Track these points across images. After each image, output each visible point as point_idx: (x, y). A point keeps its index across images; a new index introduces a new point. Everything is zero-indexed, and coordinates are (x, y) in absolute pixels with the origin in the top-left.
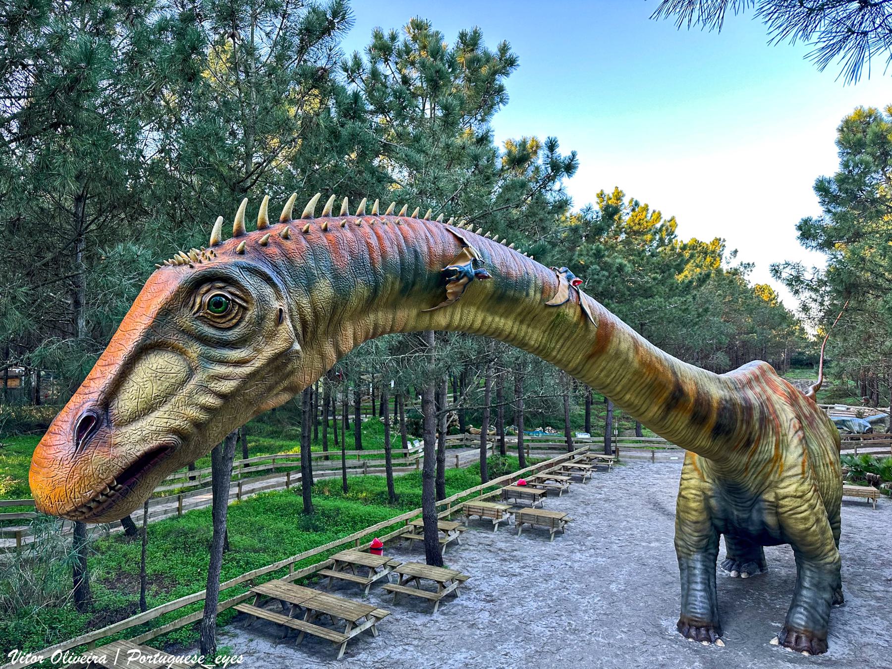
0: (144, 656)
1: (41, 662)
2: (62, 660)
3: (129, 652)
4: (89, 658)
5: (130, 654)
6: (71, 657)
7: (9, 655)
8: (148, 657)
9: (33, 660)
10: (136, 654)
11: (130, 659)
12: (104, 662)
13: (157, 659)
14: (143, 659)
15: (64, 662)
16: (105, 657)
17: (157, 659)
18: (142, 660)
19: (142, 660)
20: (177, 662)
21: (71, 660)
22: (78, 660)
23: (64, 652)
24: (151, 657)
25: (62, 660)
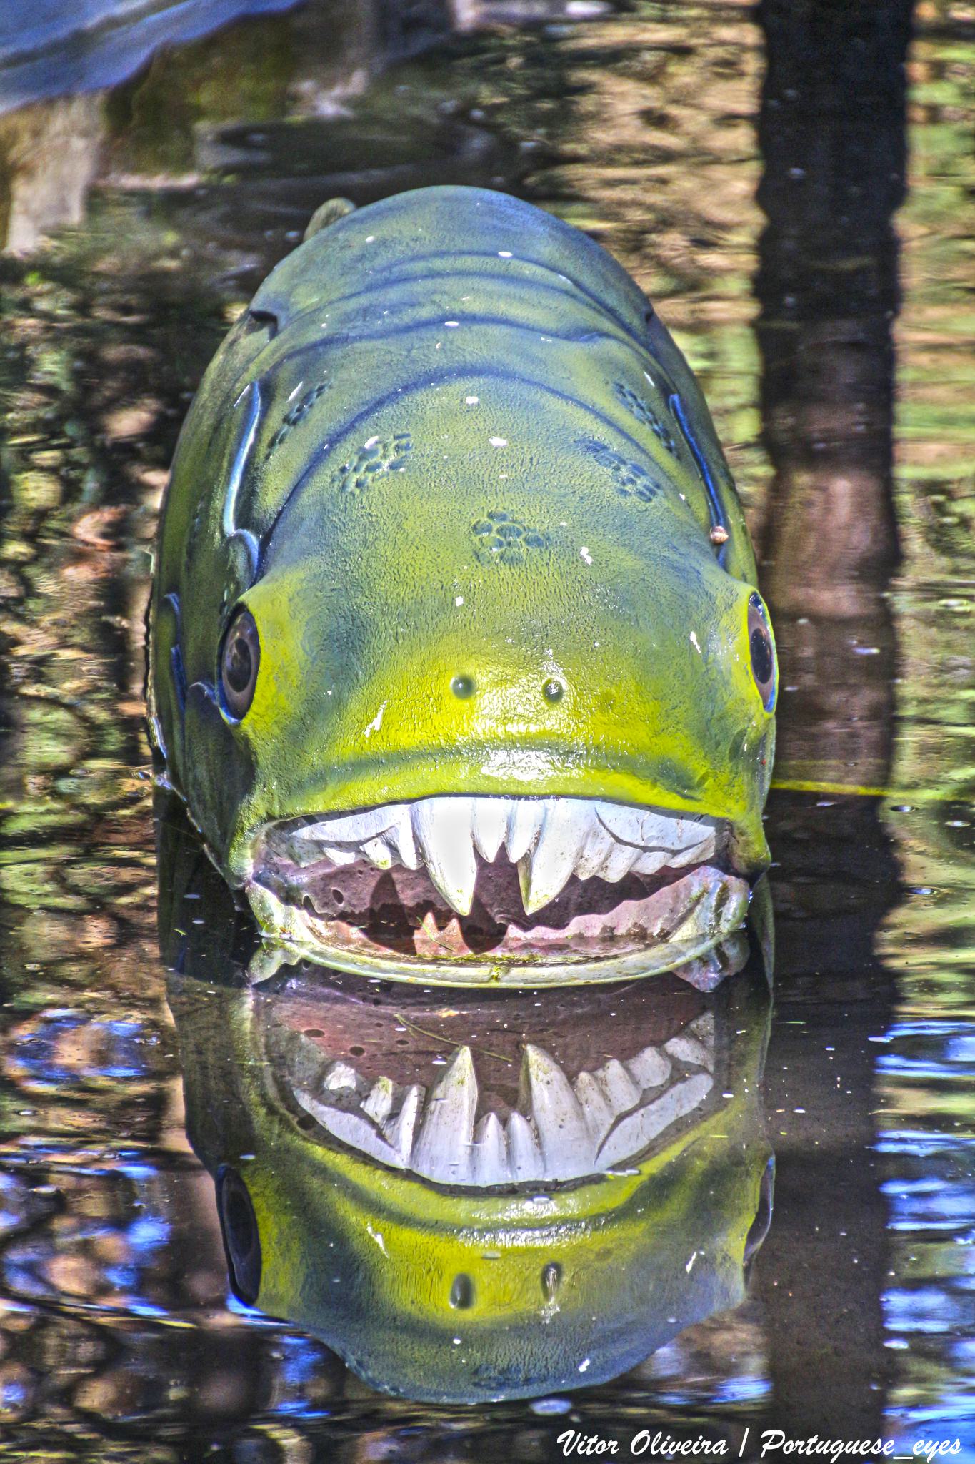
0: (791, 1442)
3: (765, 1434)
4: (697, 1443)
6: (665, 1444)
10: (778, 1439)
11: (767, 1446)
12: (723, 1452)
13: (814, 1446)
14: (791, 1446)
15: (654, 1452)
16: (723, 1442)
17: (814, 1446)
18: (788, 1449)
19: (788, 1449)
20: (848, 1452)
21: (665, 1449)
24: (802, 1443)
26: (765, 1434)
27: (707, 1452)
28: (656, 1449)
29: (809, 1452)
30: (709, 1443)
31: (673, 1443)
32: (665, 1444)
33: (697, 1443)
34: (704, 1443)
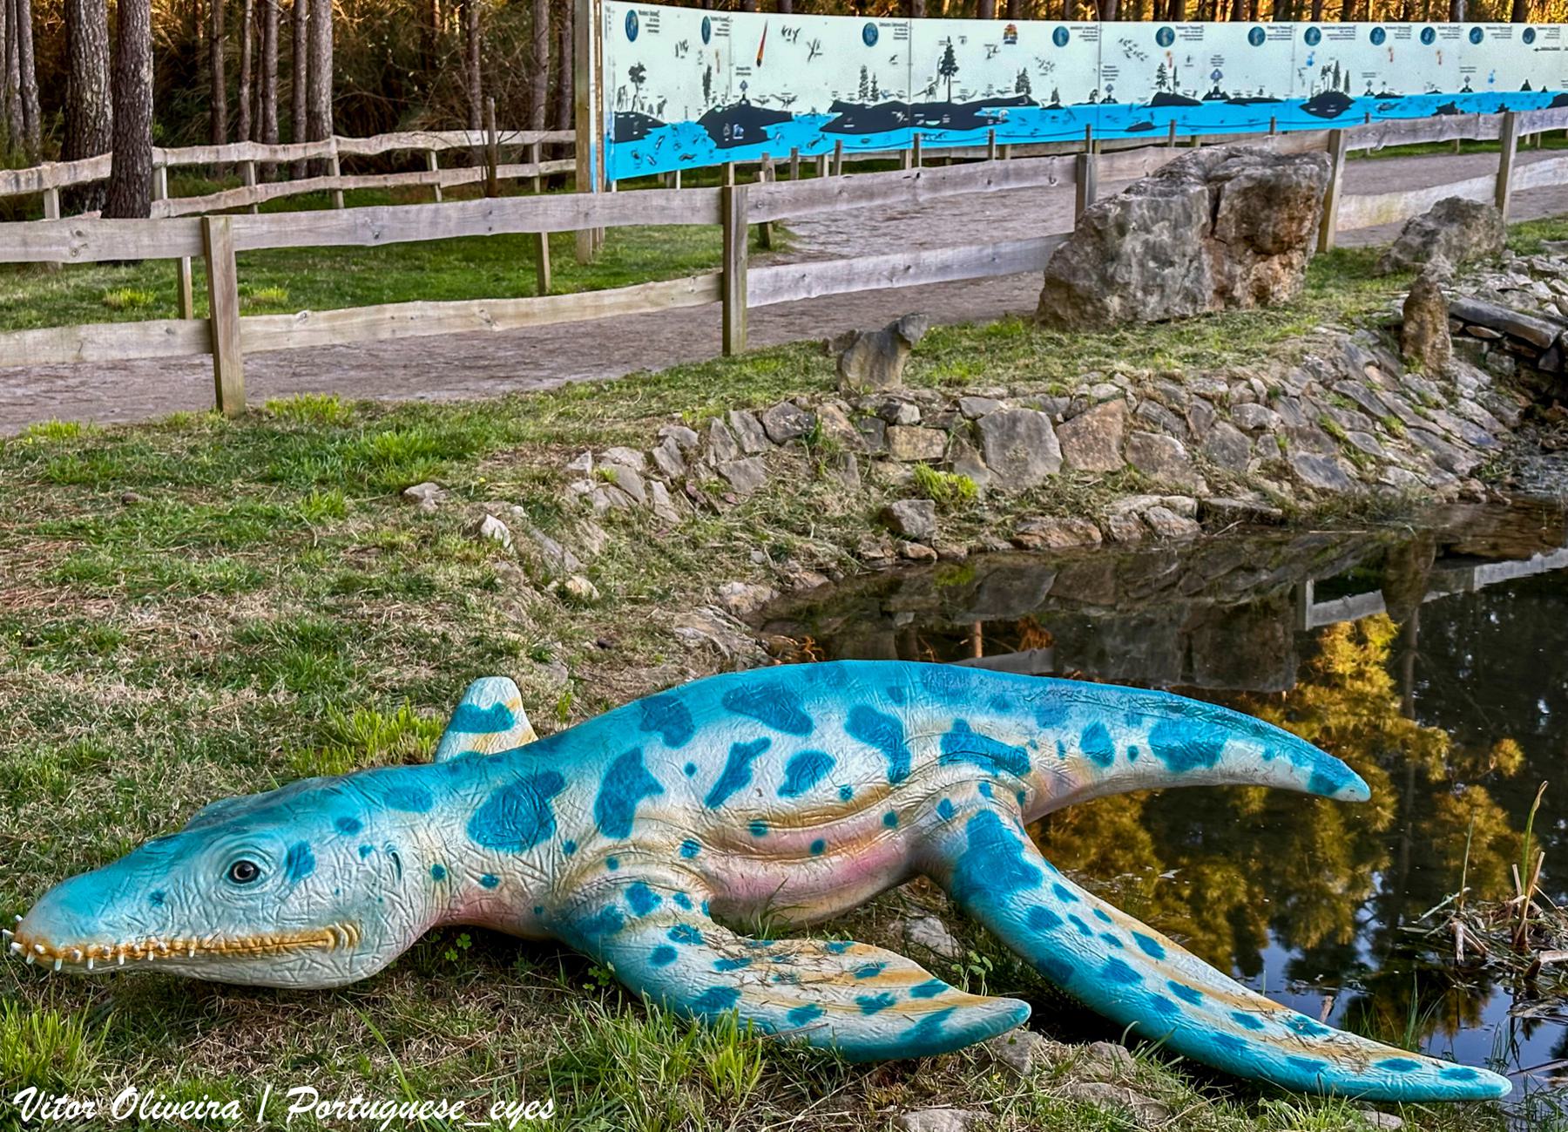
0: (326, 1103)
2: (137, 1109)
3: (292, 1092)
4: (201, 1105)
5: (297, 1096)
6: (158, 1105)
8: (337, 1104)
9: (72, 1112)
11: (294, 1109)
12: (235, 1116)
15: (143, 1117)
17: (357, 1109)
18: (322, 1112)
19: (322, 1112)
21: (160, 1110)
24: (342, 1105)
25: (137, 1109)
26: (292, 1092)
30: (216, 1105)
31: (170, 1105)
33: (201, 1105)
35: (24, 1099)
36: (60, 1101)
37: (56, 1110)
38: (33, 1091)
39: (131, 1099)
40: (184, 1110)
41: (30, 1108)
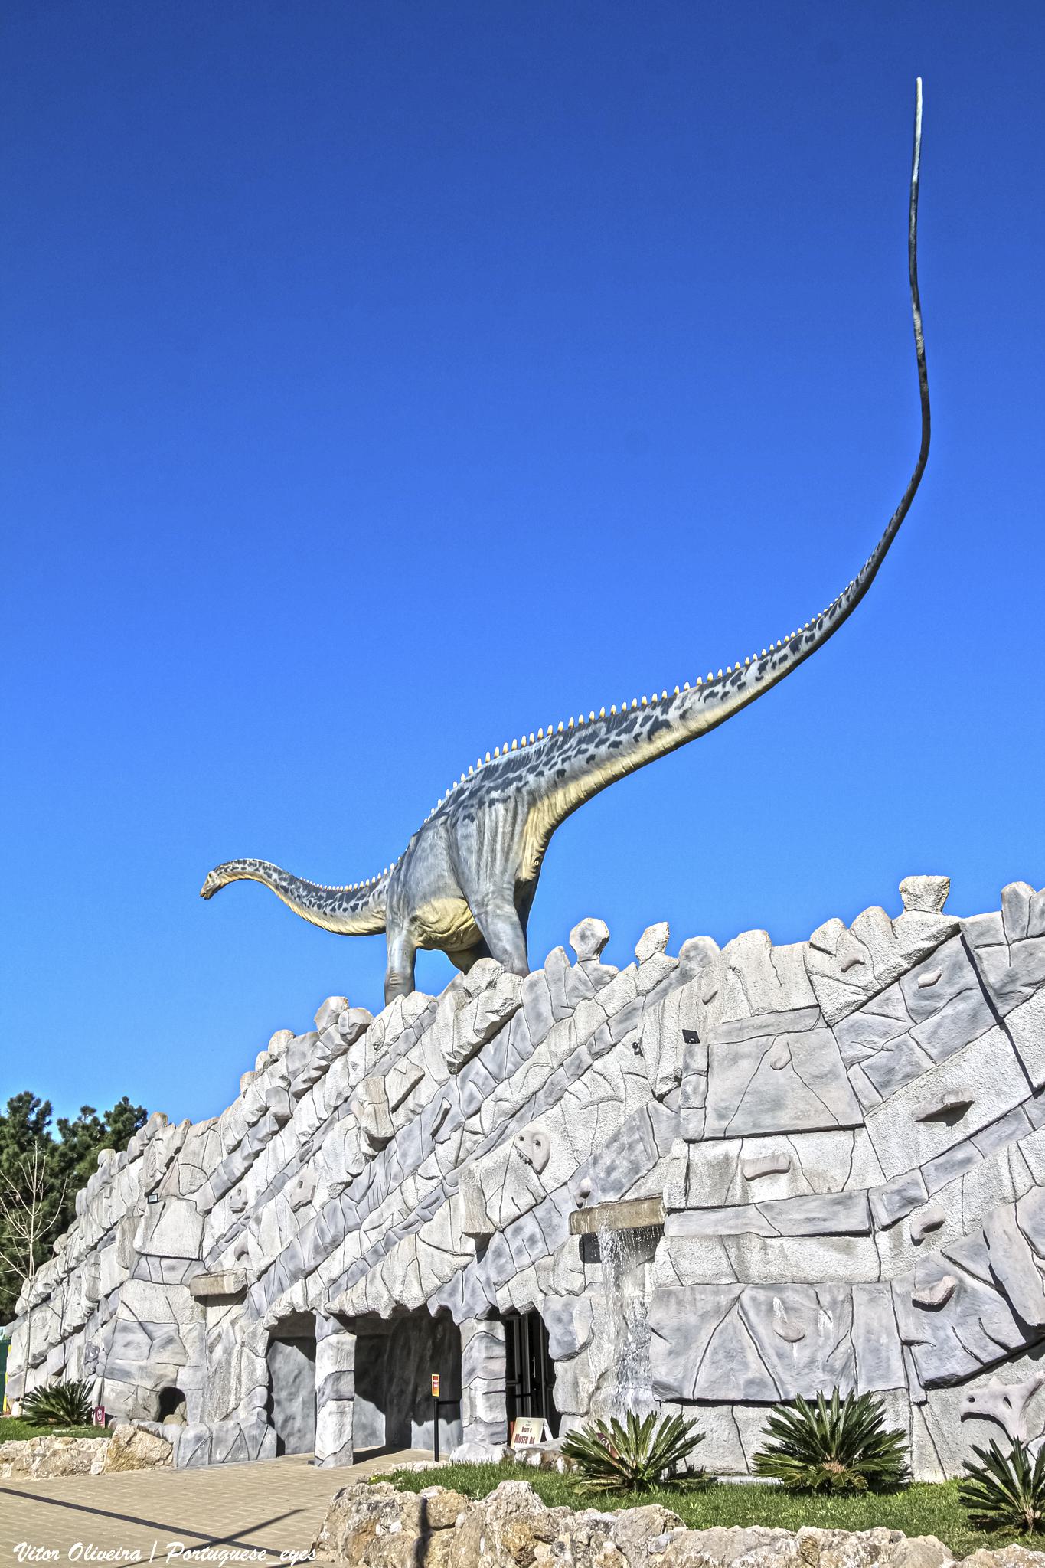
1: (56, 1559)
2: (83, 1555)
3: (169, 1545)
4: (118, 1553)
5: (172, 1548)
6: (94, 1553)
7: (15, 1550)
15: (86, 1559)
21: (95, 1556)
22: (104, 1557)
23: (85, 1545)
25: (83, 1555)
26: (169, 1545)
27: (126, 1558)
28: (89, 1554)
29: (203, 1559)
30: (128, 1552)
32: (94, 1553)
33: (118, 1553)
34: (125, 1552)
35: (20, 1549)
36: (40, 1551)
37: (37, 1556)
38: (24, 1544)
39: (79, 1549)
40: (109, 1555)
41: (23, 1556)
